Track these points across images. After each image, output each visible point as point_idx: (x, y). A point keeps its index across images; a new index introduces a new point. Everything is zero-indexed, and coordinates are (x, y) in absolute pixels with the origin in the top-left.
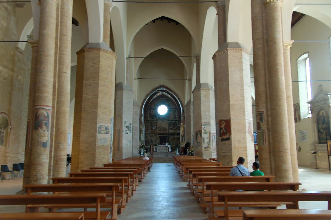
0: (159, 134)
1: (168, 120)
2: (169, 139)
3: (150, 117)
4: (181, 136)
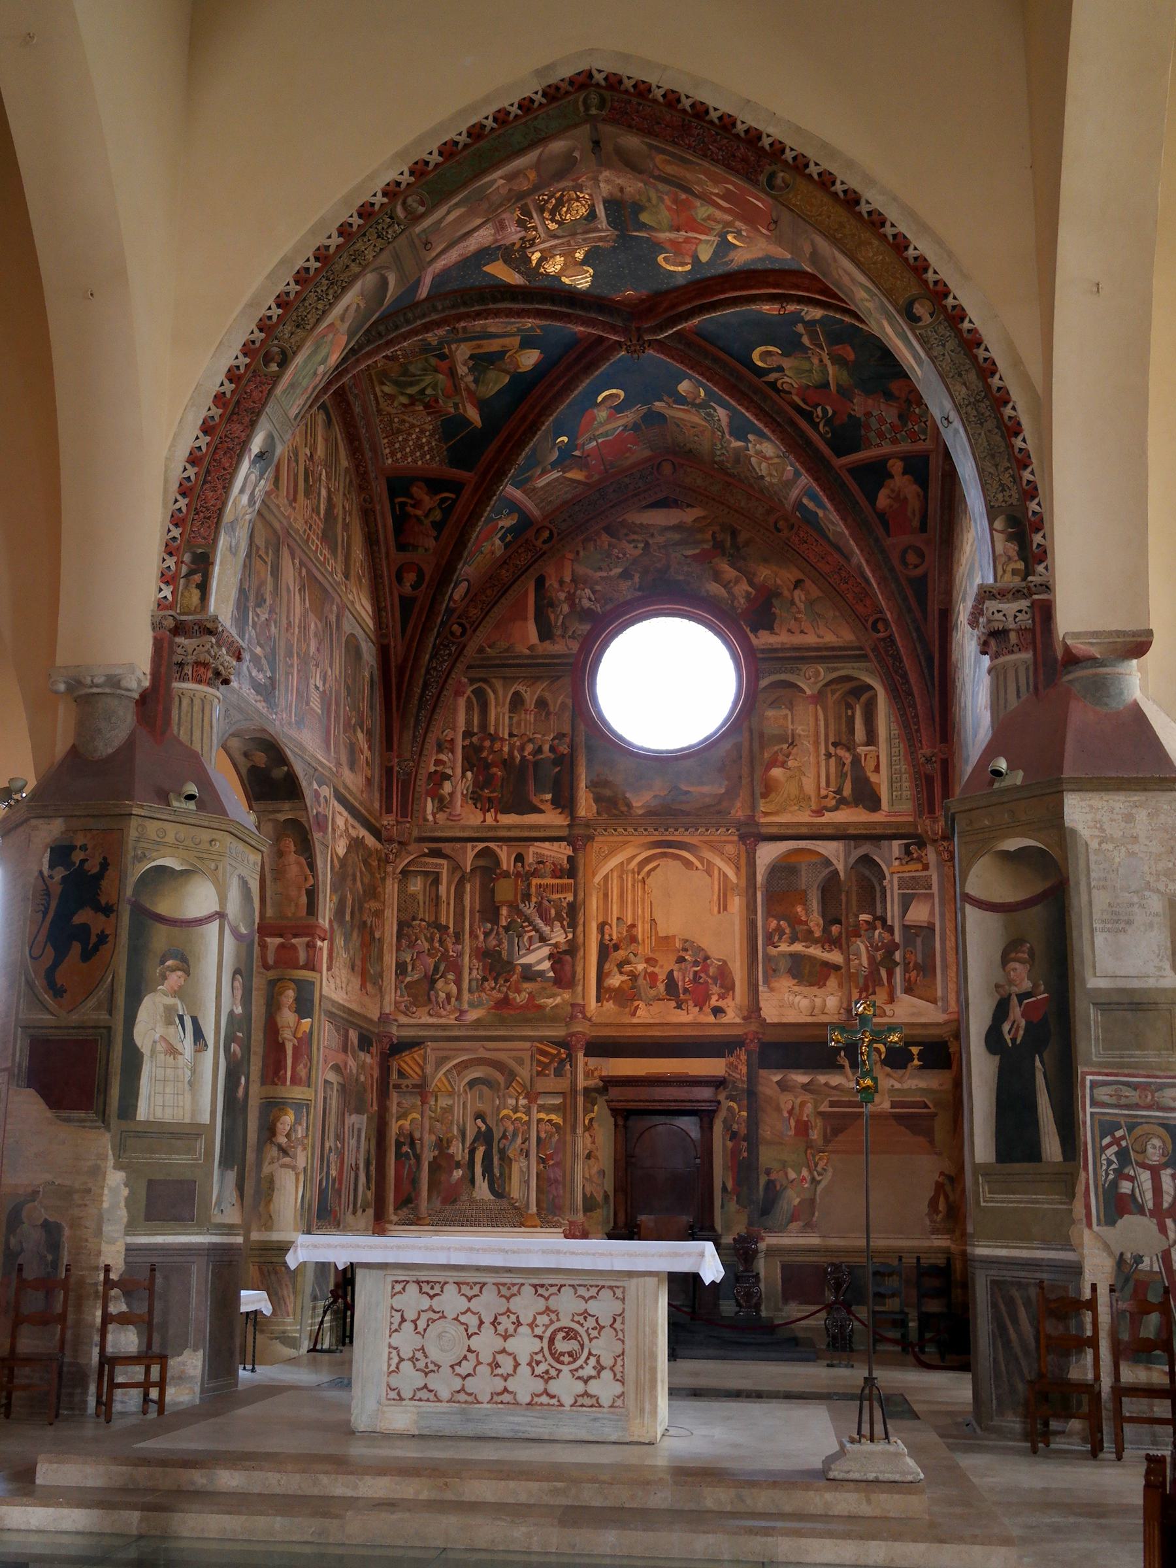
0: (602, 1048)
2: (753, 1122)
3: (475, 798)
4: (993, 1040)
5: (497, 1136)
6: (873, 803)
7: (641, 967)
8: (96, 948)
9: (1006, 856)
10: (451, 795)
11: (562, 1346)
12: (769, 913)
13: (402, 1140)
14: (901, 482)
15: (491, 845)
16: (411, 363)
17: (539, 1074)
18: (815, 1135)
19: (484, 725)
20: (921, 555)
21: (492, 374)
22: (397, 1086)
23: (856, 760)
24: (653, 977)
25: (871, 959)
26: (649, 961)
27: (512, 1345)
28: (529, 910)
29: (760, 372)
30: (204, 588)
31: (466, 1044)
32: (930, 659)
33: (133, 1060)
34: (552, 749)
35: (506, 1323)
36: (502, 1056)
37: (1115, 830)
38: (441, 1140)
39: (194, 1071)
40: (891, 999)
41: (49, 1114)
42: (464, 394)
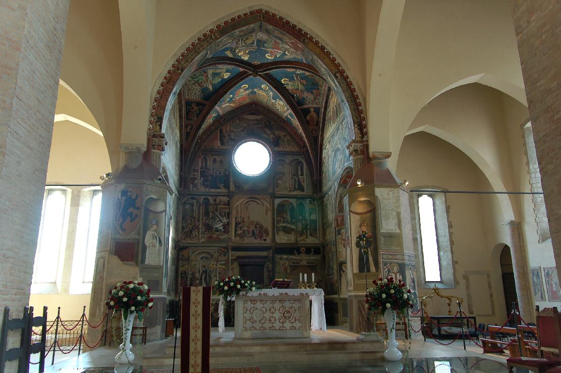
0: (235, 249)
1: (274, 197)
2: (274, 267)
3: (204, 185)
5: (208, 272)
6: (303, 190)
7: (246, 229)
8: (134, 218)
9: (361, 202)
10: (197, 183)
11: (286, 315)
12: (278, 216)
13: (183, 273)
14: (313, 113)
15: (208, 197)
17: (219, 256)
18: (288, 271)
19: (206, 166)
20: (316, 132)
22: (181, 259)
23: (299, 180)
24: (249, 231)
25: (302, 228)
26: (248, 227)
27: (274, 315)
28: (217, 214)
29: (283, 85)
30: (161, 126)
31: (200, 248)
32: (317, 156)
33: (144, 248)
34: (224, 173)
35: (272, 310)
36: (209, 251)
37: (386, 196)
38: (193, 273)
39: (159, 251)
40: (307, 238)
41: (121, 263)
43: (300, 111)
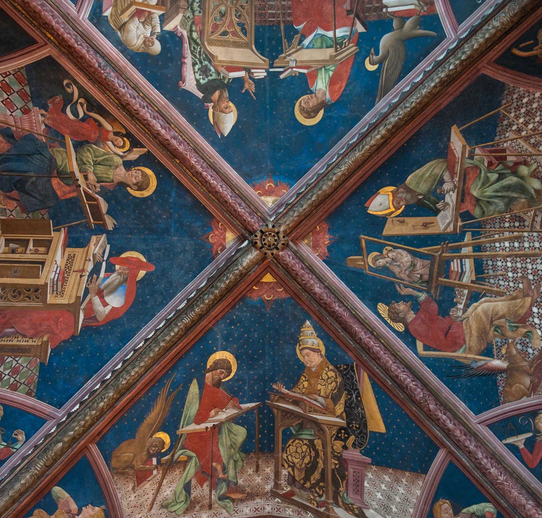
16: (500, 212)
21: (423, 188)
42: (458, 168)
43: (34, 33)
